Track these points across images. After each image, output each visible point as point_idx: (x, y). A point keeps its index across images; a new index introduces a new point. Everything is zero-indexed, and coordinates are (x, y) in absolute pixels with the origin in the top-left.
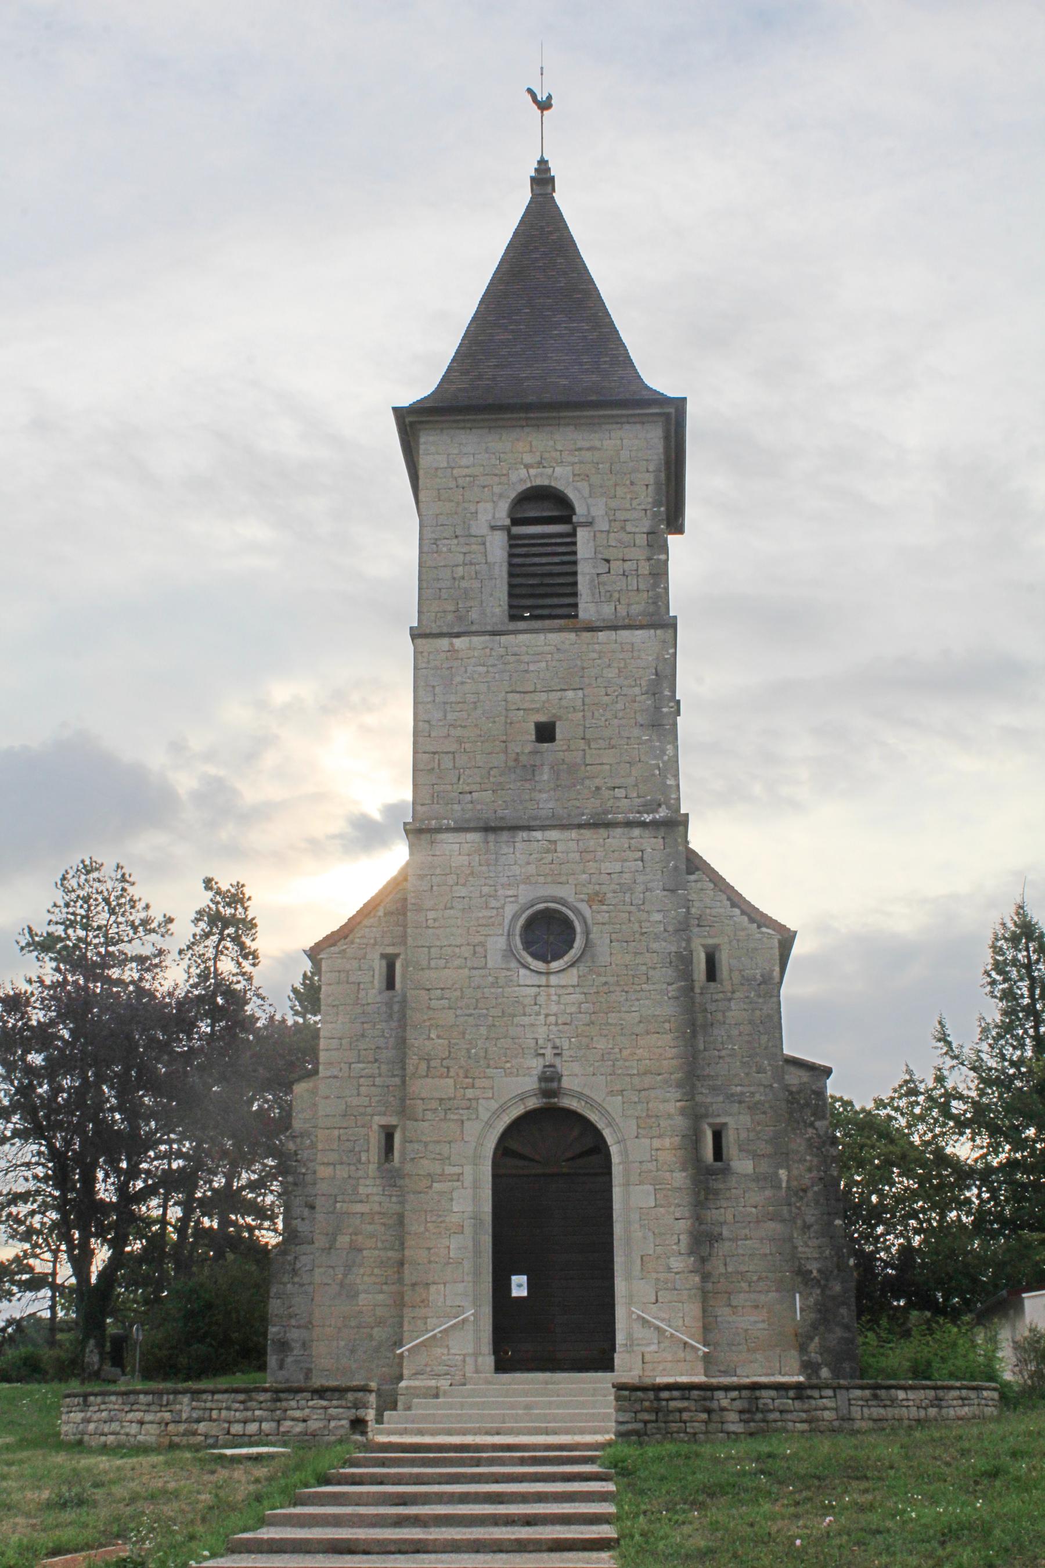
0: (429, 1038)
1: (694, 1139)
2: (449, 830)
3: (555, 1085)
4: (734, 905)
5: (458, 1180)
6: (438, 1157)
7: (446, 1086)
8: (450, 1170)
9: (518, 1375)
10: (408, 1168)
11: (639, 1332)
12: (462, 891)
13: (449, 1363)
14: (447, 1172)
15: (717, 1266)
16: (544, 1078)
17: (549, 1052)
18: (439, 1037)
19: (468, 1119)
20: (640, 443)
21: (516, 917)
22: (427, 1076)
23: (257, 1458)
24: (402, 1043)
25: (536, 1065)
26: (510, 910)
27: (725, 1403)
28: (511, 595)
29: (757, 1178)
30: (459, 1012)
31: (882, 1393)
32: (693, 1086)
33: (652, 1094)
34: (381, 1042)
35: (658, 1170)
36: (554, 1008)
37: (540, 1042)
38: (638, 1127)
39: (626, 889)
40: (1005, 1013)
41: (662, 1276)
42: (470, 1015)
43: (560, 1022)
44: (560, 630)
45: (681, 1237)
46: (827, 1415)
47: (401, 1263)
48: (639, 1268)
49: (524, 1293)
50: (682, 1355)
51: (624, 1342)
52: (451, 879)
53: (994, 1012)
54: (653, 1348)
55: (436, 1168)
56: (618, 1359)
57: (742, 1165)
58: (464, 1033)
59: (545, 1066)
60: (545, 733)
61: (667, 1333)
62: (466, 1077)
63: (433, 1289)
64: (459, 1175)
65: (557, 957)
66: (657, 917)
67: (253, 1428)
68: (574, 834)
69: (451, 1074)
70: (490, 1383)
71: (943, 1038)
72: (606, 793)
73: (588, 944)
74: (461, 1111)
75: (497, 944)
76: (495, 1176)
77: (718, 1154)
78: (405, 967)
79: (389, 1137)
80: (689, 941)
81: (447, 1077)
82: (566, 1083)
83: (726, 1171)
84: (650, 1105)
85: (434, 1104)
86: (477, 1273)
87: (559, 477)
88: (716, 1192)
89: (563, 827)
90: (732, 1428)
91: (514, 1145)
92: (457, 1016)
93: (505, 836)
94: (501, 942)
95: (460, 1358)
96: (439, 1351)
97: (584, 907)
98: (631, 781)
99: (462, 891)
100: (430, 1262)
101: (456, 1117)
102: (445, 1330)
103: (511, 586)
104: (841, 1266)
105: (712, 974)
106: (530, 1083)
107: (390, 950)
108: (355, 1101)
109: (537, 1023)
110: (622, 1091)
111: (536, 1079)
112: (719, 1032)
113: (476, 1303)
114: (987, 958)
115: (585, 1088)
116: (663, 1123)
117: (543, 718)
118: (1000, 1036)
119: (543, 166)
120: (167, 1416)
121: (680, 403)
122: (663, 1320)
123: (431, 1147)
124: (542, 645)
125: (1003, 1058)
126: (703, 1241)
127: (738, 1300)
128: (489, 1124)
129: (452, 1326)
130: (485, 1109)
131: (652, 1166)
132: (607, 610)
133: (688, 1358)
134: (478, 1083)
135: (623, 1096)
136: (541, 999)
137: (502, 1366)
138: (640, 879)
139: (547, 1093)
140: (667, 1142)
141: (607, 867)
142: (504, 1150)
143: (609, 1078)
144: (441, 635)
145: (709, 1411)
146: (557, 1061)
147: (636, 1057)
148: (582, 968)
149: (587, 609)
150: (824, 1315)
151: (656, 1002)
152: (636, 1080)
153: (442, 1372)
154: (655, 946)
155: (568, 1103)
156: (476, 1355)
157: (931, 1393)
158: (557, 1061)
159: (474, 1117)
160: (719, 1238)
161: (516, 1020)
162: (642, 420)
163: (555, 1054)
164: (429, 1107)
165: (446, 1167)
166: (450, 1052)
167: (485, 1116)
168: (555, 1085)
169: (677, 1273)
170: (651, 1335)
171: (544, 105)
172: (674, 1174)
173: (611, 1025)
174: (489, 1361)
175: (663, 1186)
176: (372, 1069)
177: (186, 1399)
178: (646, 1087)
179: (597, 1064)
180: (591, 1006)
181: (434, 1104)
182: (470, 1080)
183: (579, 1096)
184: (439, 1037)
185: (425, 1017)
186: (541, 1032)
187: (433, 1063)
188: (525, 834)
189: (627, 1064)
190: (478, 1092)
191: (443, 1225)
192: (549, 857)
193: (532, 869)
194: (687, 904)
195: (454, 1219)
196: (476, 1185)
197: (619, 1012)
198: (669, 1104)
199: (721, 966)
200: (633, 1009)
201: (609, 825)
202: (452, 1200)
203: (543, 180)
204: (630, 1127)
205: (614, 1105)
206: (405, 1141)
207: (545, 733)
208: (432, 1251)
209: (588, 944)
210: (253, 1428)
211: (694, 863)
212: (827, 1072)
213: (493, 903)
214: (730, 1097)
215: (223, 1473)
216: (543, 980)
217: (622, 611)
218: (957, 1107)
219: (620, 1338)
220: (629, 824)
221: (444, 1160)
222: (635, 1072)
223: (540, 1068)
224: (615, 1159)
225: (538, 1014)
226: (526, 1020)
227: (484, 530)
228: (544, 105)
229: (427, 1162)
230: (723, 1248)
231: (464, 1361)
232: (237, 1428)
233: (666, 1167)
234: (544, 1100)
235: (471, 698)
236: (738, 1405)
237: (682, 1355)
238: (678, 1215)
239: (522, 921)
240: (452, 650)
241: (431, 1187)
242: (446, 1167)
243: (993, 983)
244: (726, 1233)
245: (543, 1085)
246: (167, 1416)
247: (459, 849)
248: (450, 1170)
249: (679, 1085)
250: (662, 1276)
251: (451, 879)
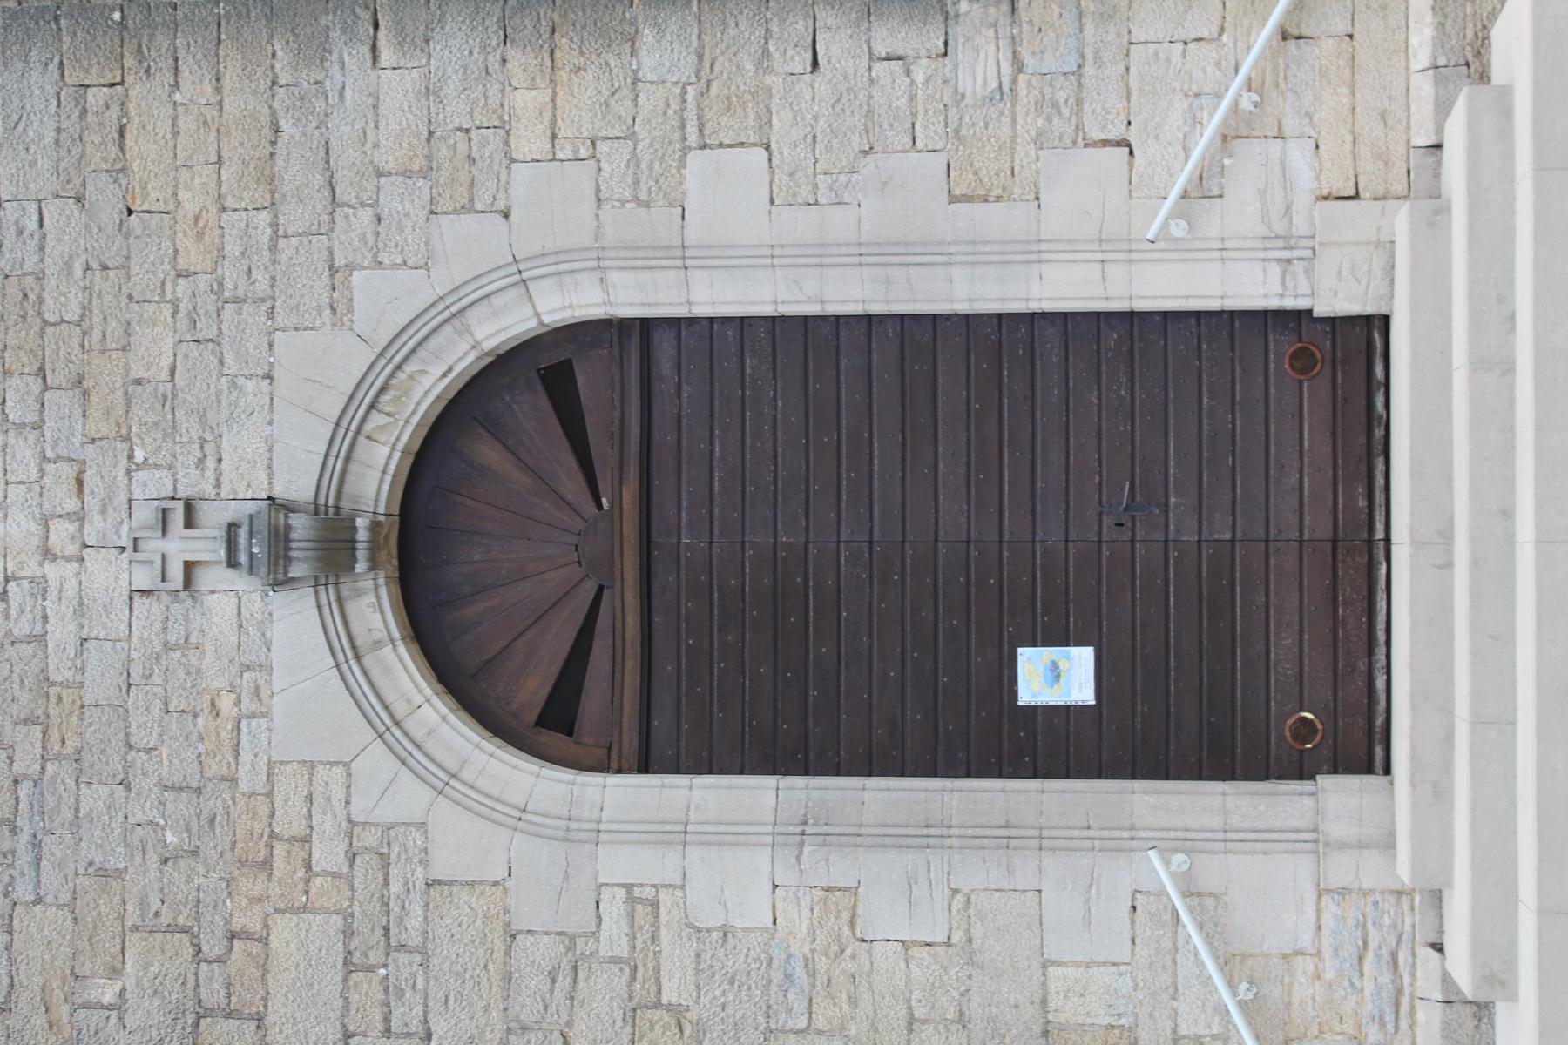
0: (119, 1006)
3: (301, 525)
5: (655, 905)
6: (564, 982)
7: (301, 946)
8: (614, 937)
11: (1240, 211)
13: (1350, 950)
14: (623, 950)
17: (179, 546)
18: (115, 972)
19: (425, 863)
22: (259, 1019)
25: (229, 595)
30: (23, 891)
33: (346, 158)
35: (632, 136)
37: (144, 578)
38: (468, 209)
41: (1029, 123)
42: (36, 844)
43: (71, 504)
45: (881, 49)
48: (994, 209)
49: (1083, 657)
50: (1328, 45)
51: (1275, 269)
54: (1298, 155)
56: (1335, 298)
58: (103, 873)
59: (232, 563)
61: (1246, 104)
62: (267, 865)
63: (1065, 1010)
64: (632, 900)
69: (254, 925)
70: (1437, 794)
74: (395, 888)
81: (265, 941)
82: (298, 484)
84: (388, 161)
85: (367, 989)
86: (1008, 836)
91: (533, 689)
92: (39, 900)
95: (1330, 906)
96: (1304, 990)
100: (962, 1020)
101: (417, 909)
102: (1224, 964)
106: (294, 620)
109: (71, 588)
110: (333, 270)
111: (279, 599)
115: (317, 407)
116: (455, 112)
122: (1196, 122)
123: (529, 1013)
128: (445, 781)
129: (1209, 939)
131: (615, 158)
133: (1342, 26)
134: (289, 821)
135: (351, 267)
139: (335, 549)
140: (527, 101)
142: (553, 726)
143: (280, 320)
146: (214, 516)
147: (211, 216)
152: (294, 216)
153: (1386, 978)
155: (375, 482)
156: (1316, 843)
158: (214, 516)
159: (416, 836)
161: (60, 670)
163: (189, 524)
164: (377, 1015)
165: (604, 951)
166: (170, 929)
167: (411, 798)
168: (301, 525)
169: (1019, 66)
170: (1250, 167)
172: (647, 73)
173: (86, 309)
174: (1339, 795)
175: (691, 115)
178: (318, 180)
179: (232, 367)
180: (16, 381)
181: (367, 989)
182: (279, 849)
183: (346, 437)
184: (115, 972)
185: (40, 1021)
186: (108, 575)
187: (213, 995)
189: (233, 248)
190: (326, 824)
191: (822, 964)
195: (797, 917)
196: (679, 835)
197: (40, 277)
200: (32, 224)
202: (726, 932)
204: (468, 245)
205: (385, 300)
208: (919, 1013)
219: (1252, 287)
221: (575, 959)
222: (264, 217)
223: (241, 581)
225: (40, 587)
226: (61, 632)
229: (580, 1027)
231: (1343, 892)
233: (622, 107)
234: (361, 567)
237: (1328, 45)
238: (803, 60)
241: (677, 1011)
242: (604, 951)
245: (296, 571)
248: (614, 937)
249: (317, 51)
250: (1029, 123)
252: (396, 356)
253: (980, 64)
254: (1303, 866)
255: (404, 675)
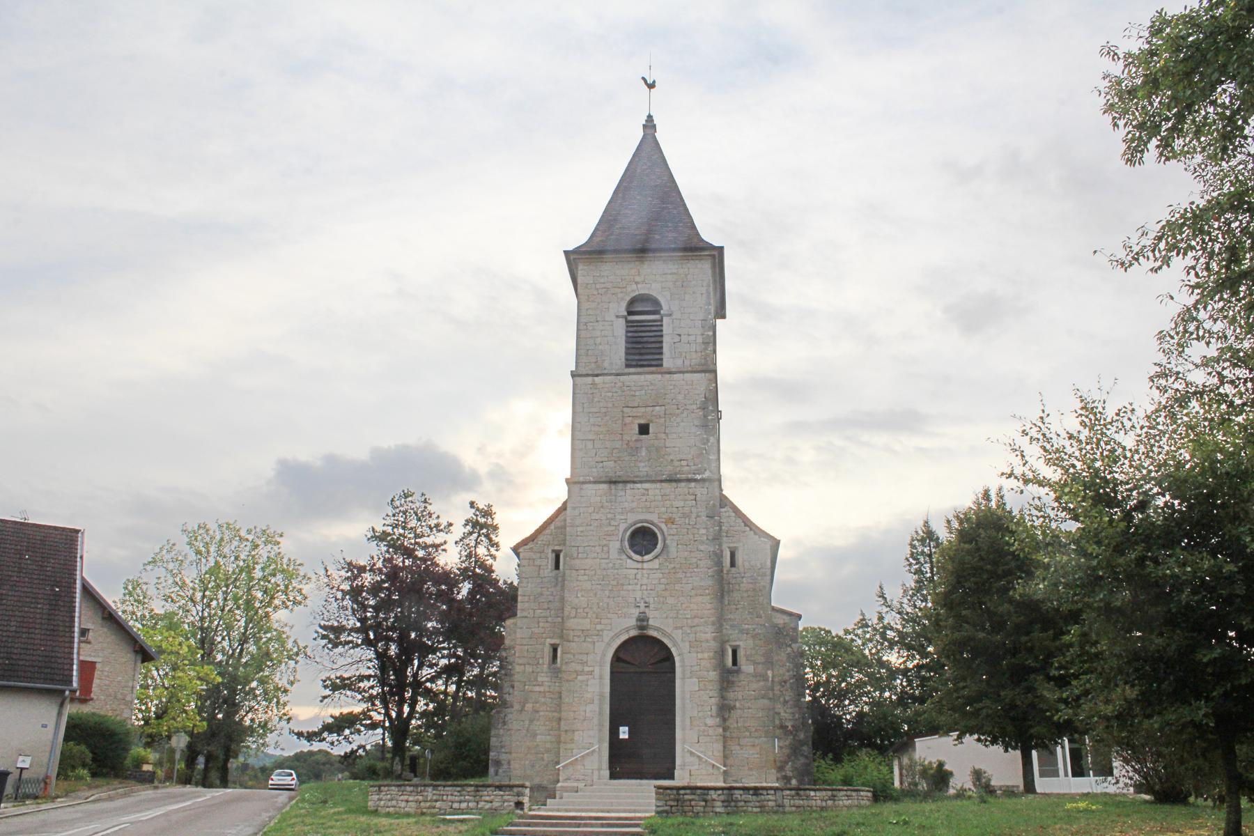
1: (722, 653)
2: (590, 482)
4: (746, 525)
8: (587, 669)
9: (622, 781)
10: (564, 667)
11: (689, 759)
12: (595, 516)
15: (731, 723)
16: (639, 620)
17: (642, 605)
20: (701, 270)
21: (625, 531)
23: (462, 821)
24: (562, 599)
26: (622, 527)
27: (715, 797)
28: (627, 354)
29: (755, 675)
31: (802, 793)
32: (721, 625)
34: (551, 598)
36: (645, 581)
39: (685, 516)
40: (917, 582)
44: (653, 373)
46: (770, 803)
47: (560, 719)
52: (591, 510)
53: (911, 581)
55: (579, 668)
56: (676, 773)
57: (747, 667)
60: (644, 429)
65: (647, 553)
66: (704, 531)
67: (464, 805)
68: (658, 485)
71: (882, 596)
72: (677, 463)
73: (665, 546)
75: (615, 545)
76: (612, 673)
77: (735, 662)
78: (565, 557)
79: (555, 650)
80: (720, 545)
82: (651, 622)
83: (738, 671)
87: (654, 290)
88: (733, 682)
89: (653, 482)
90: (718, 810)
91: (621, 655)
93: (620, 486)
94: (618, 545)
97: (663, 526)
98: (690, 457)
99: (595, 516)
103: (627, 348)
104: (804, 724)
105: (733, 564)
106: (633, 622)
107: (557, 548)
108: (536, 631)
112: (736, 595)
113: (600, 741)
114: (908, 550)
115: (662, 626)
117: (643, 422)
118: (914, 595)
119: (650, 118)
120: (421, 798)
121: (721, 250)
124: (643, 380)
125: (915, 606)
126: (725, 709)
127: (743, 742)
128: (609, 644)
130: (607, 636)
132: (679, 362)
136: (639, 576)
137: (613, 776)
138: (694, 510)
139: (641, 628)
140: (706, 655)
141: (677, 504)
142: (617, 659)
144: (587, 375)
145: (706, 801)
148: (661, 559)
149: (667, 362)
150: (795, 750)
151: (702, 578)
154: (702, 548)
156: (599, 769)
157: (830, 793)
160: (734, 708)
162: (700, 258)
167: (606, 640)
171: (651, 86)
174: (607, 773)
176: (546, 613)
177: (430, 789)
183: (657, 629)
186: (638, 595)
188: (631, 485)
192: (644, 498)
193: (634, 505)
194: (720, 524)
195: (589, 696)
196: (601, 677)
198: (708, 634)
199: (734, 559)
201: (678, 481)
203: (650, 125)
204: (685, 647)
205: (677, 635)
206: (563, 653)
207: (644, 429)
209: (665, 546)
210: (464, 805)
211: (724, 502)
212: (799, 617)
213: (613, 523)
214: (742, 631)
215: (443, 828)
216: (639, 566)
217: (687, 363)
218: (890, 634)
219: (678, 762)
220: (689, 480)
221: (584, 663)
224: (677, 664)
227: (613, 318)
228: (651, 86)
230: (735, 714)
232: (456, 805)
235: (603, 410)
236: (722, 798)
239: (628, 533)
240: (593, 384)
243: (910, 565)
244: (738, 705)
246: (421, 798)
247: (595, 492)
249: (713, 624)
251: (591, 510)
252: (669, 636)
253: (710, 721)
254: (596, 767)
255: (624, 637)
